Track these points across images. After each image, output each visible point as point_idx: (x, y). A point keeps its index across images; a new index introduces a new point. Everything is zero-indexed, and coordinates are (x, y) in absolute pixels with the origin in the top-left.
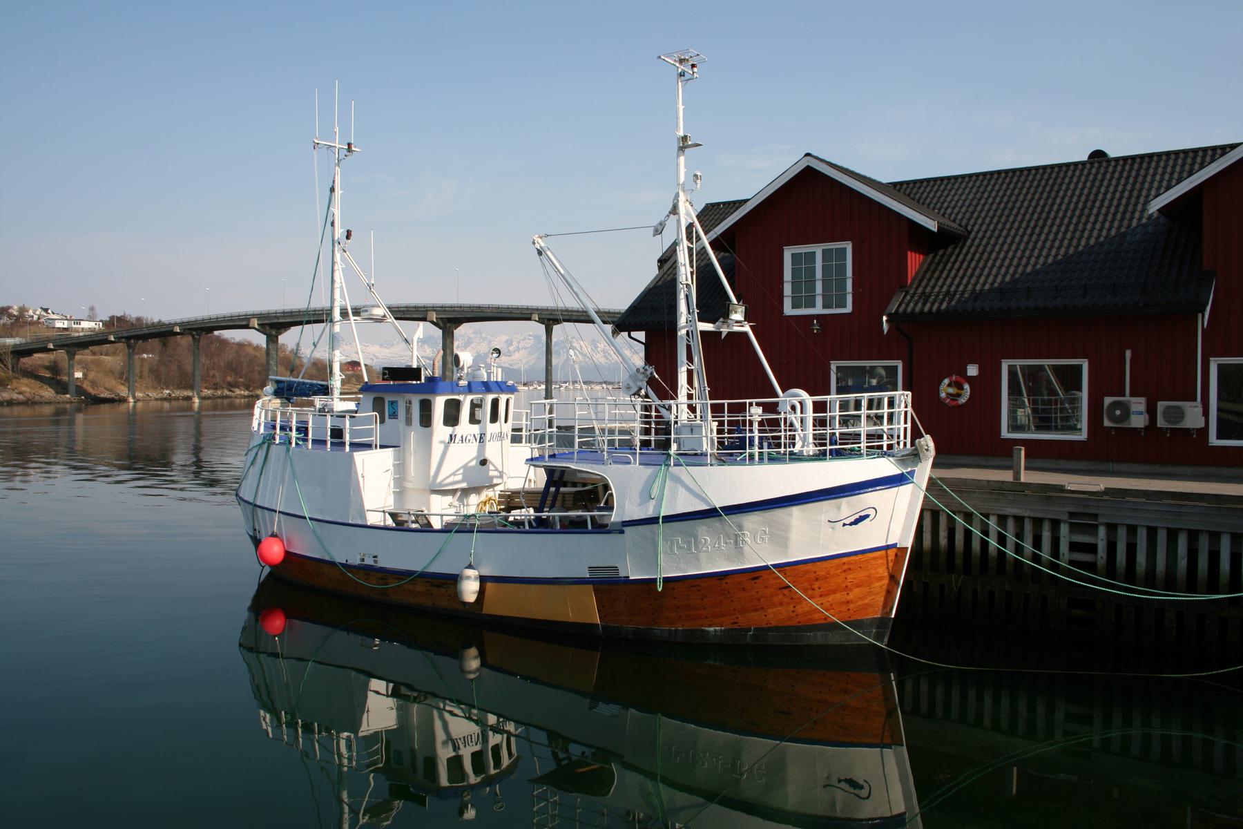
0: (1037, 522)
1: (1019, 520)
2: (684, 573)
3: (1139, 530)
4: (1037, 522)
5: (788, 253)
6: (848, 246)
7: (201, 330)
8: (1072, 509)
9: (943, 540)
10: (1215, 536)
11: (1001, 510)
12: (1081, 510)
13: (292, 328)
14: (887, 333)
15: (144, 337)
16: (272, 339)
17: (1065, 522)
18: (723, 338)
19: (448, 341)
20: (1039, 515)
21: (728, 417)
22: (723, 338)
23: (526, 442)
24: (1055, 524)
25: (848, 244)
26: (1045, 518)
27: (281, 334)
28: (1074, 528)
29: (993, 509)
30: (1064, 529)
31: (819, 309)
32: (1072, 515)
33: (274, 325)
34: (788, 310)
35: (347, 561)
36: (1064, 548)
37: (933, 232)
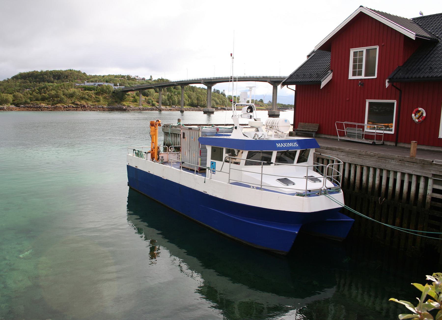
0: (418, 177)
1: (410, 175)
2: (309, 198)
3: (377, 169)
4: (418, 177)
5: (352, 51)
6: (377, 47)
7: (184, 84)
8: (434, 173)
9: (377, 182)
10: (395, 173)
11: (402, 170)
12: (438, 173)
13: (217, 84)
14: (387, 88)
15: (163, 87)
16: (210, 88)
17: (431, 178)
18: (322, 87)
19: (275, 90)
20: (411, 173)
21: (356, 129)
22: (322, 87)
23: (274, 134)
24: (426, 179)
25: (377, 47)
26: (421, 176)
27: (212, 86)
28: (435, 182)
29: (398, 169)
30: (430, 182)
31: (363, 77)
32: (434, 175)
33: (210, 83)
34: (351, 77)
35: (129, 164)
36: (429, 192)
37: (414, 40)
